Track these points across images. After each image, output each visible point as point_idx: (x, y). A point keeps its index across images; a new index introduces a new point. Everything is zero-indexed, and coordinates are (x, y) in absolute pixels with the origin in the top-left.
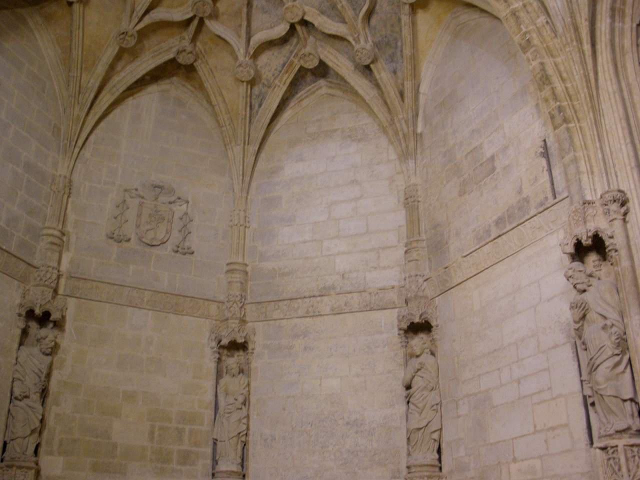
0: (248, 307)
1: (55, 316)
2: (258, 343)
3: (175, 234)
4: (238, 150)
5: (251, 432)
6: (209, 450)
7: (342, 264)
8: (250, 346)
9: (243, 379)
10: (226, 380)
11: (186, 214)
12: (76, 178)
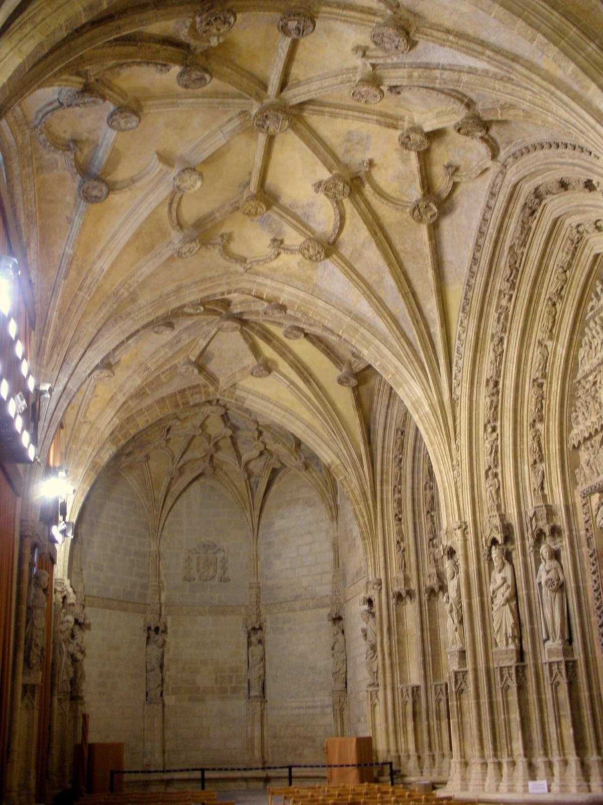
1: (162, 628)
2: (268, 626)
3: (220, 572)
4: (248, 514)
5: (267, 674)
6: (246, 685)
8: (264, 629)
9: (260, 647)
10: (252, 648)
11: (224, 558)
12: (162, 549)
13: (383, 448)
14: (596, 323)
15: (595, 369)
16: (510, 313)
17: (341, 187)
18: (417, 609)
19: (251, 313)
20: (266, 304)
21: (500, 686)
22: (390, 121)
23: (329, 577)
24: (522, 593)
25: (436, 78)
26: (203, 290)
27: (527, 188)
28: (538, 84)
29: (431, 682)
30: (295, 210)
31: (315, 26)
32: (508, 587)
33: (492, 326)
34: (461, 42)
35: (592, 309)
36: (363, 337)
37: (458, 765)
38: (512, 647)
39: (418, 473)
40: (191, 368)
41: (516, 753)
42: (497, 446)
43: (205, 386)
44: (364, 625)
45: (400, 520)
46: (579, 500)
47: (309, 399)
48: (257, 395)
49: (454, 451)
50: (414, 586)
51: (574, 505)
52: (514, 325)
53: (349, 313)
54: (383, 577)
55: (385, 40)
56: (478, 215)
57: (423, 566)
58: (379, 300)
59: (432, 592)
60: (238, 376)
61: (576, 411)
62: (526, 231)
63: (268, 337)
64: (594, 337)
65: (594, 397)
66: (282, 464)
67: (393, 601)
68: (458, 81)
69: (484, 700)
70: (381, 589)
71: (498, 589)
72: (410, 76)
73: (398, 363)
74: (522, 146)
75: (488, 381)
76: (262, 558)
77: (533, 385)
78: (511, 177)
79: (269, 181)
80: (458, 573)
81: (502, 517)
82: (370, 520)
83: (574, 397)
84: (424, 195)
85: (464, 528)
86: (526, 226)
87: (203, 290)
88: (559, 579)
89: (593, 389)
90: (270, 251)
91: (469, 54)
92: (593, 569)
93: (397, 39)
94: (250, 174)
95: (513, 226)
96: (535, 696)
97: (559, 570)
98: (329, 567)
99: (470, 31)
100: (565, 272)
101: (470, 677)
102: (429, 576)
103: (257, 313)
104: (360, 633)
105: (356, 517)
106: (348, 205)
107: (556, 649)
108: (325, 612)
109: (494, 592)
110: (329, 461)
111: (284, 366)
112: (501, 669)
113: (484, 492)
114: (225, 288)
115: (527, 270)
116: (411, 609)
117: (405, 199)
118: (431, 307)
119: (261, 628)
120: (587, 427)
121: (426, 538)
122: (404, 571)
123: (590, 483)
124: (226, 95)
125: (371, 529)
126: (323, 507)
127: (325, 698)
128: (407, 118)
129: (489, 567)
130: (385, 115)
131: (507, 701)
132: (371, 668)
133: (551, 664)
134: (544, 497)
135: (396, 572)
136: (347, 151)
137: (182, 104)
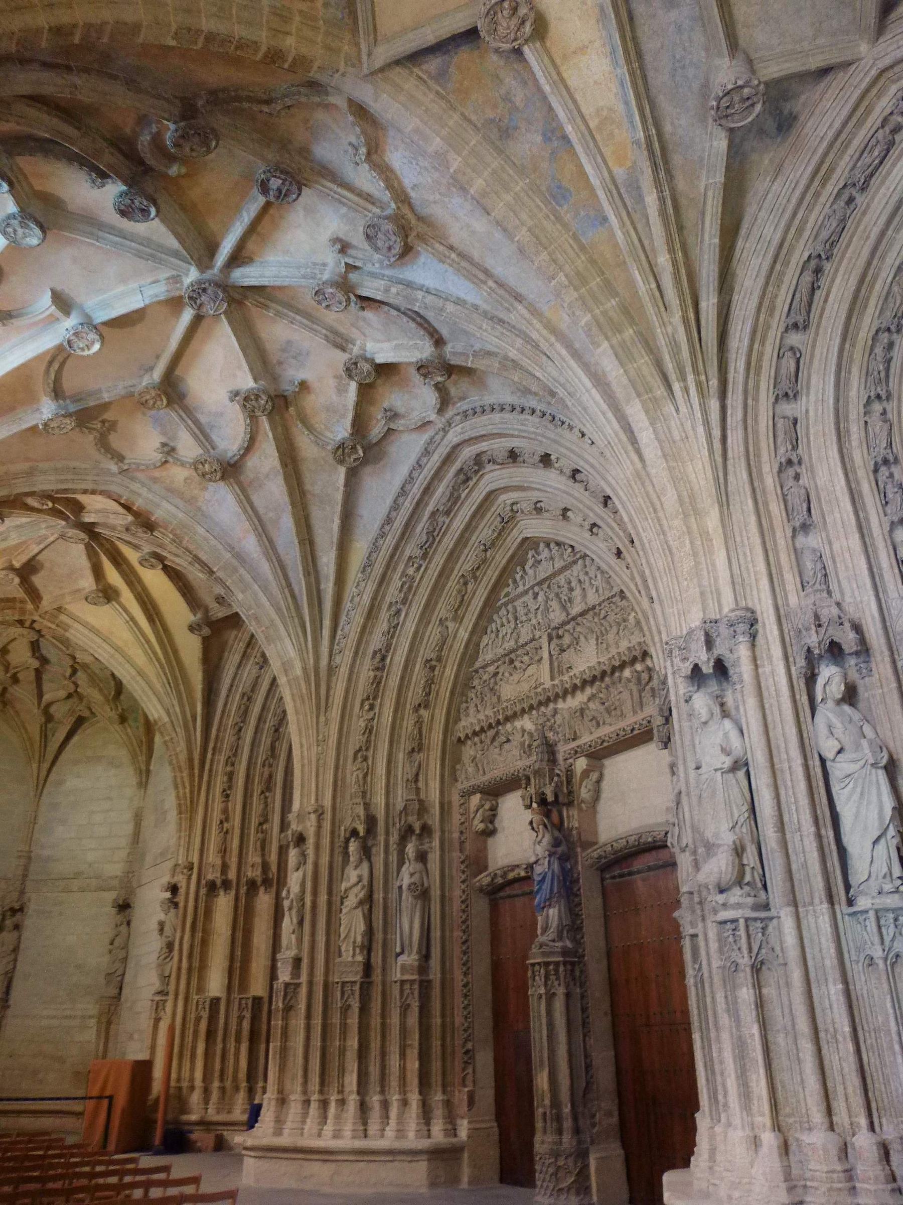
0: (28, 883)
2: (32, 907)
4: (35, 766)
7: (90, 857)
9: (15, 934)
13: (223, 711)
14: (508, 612)
15: (499, 659)
16: (415, 584)
17: (263, 402)
18: (232, 903)
19: (105, 525)
20: (130, 518)
21: (339, 1005)
22: (339, 340)
23: (123, 854)
24: (379, 896)
25: (417, 300)
26: (62, 481)
27: (468, 453)
28: (538, 331)
29: (235, 996)
30: (199, 416)
31: (299, 195)
32: (364, 887)
33: (393, 593)
34: (464, 264)
35: (506, 596)
36: (241, 580)
37: (273, 1103)
38: (359, 958)
39: (259, 747)
40: (11, 576)
41: (347, 1089)
42: (372, 727)
43: (22, 601)
44: (162, 916)
45: (227, 796)
46: (456, 799)
47: (148, 641)
48: (85, 625)
49: (322, 724)
50: (232, 875)
51: (450, 803)
52: (417, 597)
53: (231, 548)
54: (196, 860)
55: (380, 235)
56: (403, 471)
57: (247, 854)
58: (271, 541)
59: (252, 886)
60: (68, 599)
61: (467, 702)
62: (454, 500)
63: (118, 560)
64: (503, 625)
65: (492, 689)
66: (92, 713)
67: (203, 891)
68: (442, 310)
69: (317, 1021)
70: (191, 875)
71: (351, 888)
72: (387, 290)
73: (274, 616)
74: (478, 404)
75: (375, 652)
76: (41, 821)
77: (425, 666)
78: (453, 437)
79: (178, 372)
80: (305, 863)
81: (367, 806)
82: (192, 792)
83: (467, 685)
84: (352, 435)
85: (320, 813)
86: (456, 494)
87: (62, 481)
88: (423, 885)
89: (492, 681)
90: (158, 457)
91: (470, 280)
92: (463, 877)
93: (393, 238)
94: (158, 357)
95: (441, 490)
96: (379, 1020)
97: (424, 874)
98: (124, 842)
99: (476, 255)
100: (486, 550)
101: (304, 990)
102: (253, 866)
103: (113, 528)
104: (154, 926)
105: (176, 787)
106: (265, 423)
107: (411, 965)
108: (111, 896)
109: (346, 891)
110: (156, 716)
111: (127, 596)
112: (344, 983)
113: (348, 776)
114: (90, 486)
115: (445, 541)
116: (223, 904)
117: (329, 435)
118: (327, 561)
119: (21, 909)
120: (479, 720)
121: (254, 821)
122: (223, 857)
123: (473, 782)
124: (161, 248)
125: (192, 802)
126: (131, 771)
127: (89, 1007)
128: (358, 343)
129: (343, 861)
130: (336, 333)
131: (345, 1024)
132: (163, 971)
133: (403, 982)
134: (418, 790)
135: (213, 857)
136: (280, 363)
137: (104, 239)
